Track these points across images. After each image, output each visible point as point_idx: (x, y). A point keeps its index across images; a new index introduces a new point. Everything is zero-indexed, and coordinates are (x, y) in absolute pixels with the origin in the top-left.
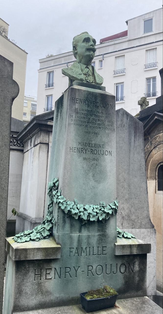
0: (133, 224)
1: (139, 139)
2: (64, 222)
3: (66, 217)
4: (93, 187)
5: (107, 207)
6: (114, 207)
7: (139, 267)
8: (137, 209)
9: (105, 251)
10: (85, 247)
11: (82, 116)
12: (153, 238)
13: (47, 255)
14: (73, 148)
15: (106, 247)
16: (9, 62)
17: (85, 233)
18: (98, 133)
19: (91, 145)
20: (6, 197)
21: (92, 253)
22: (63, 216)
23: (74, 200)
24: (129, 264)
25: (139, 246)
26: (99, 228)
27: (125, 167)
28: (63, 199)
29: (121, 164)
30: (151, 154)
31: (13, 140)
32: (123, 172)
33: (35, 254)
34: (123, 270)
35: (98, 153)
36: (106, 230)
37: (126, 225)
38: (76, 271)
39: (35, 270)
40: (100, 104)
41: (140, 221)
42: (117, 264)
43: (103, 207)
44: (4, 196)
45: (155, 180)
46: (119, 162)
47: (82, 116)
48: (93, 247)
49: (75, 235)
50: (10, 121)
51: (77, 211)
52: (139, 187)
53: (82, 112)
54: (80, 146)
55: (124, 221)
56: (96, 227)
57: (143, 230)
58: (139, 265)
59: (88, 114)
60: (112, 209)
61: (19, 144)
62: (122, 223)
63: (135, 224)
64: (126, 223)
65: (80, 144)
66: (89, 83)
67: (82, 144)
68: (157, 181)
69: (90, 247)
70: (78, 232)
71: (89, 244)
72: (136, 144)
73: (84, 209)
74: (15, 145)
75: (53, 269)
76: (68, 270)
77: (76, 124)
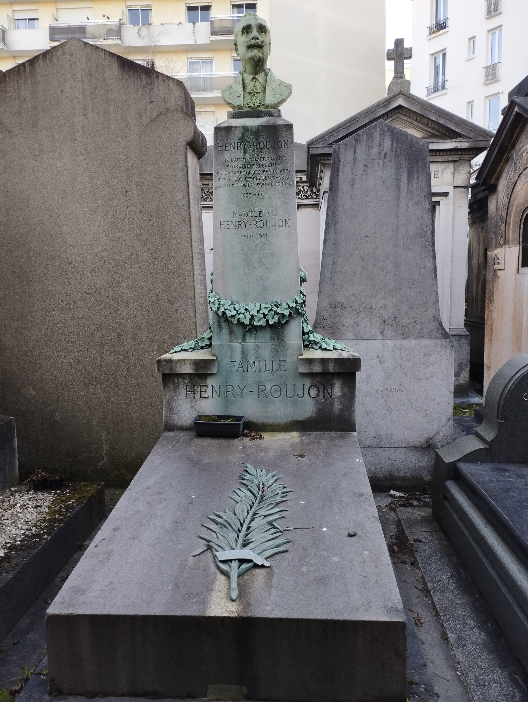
0: (404, 333)
1: (418, 176)
2: (220, 327)
3: (222, 321)
4: (260, 278)
5: (283, 306)
6: (294, 305)
7: (342, 391)
8: (413, 307)
9: (283, 366)
10: (252, 361)
11: (237, 169)
12: (447, 356)
13: (196, 370)
14: (225, 222)
15: (285, 361)
16: (176, 82)
17: (251, 342)
18: (264, 193)
19: (253, 214)
20: (193, 297)
21: (263, 368)
22: (218, 320)
23: (232, 298)
24: (324, 385)
25: (339, 361)
26: (273, 336)
27: (387, 234)
28: (214, 297)
29: (379, 228)
30: (515, 190)
31: (303, 187)
32: (383, 243)
33: (182, 367)
34: (313, 393)
35: (265, 225)
36: (285, 338)
37: (389, 333)
38: (242, 391)
39: (187, 386)
40: (265, 145)
41: (418, 327)
42: (303, 385)
43: (276, 305)
44: (190, 295)
45: (518, 245)
46: (375, 226)
47: (237, 169)
48: (265, 361)
49: (237, 345)
50: (186, 182)
51: (234, 313)
52: (418, 267)
53: (236, 163)
54: (236, 219)
55: (386, 327)
56: (267, 334)
57: (424, 342)
58: (342, 388)
59: (246, 165)
60: (289, 308)
61: (315, 193)
62: (382, 331)
63: (407, 331)
64: (390, 331)
65: (236, 215)
66: (253, 108)
67: (238, 215)
68: (521, 247)
69: (260, 361)
70: (240, 341)
71: (258, 356)
72: (412, 186)
73: (246, 309)
74: (308, 196)
75: (210, 387)
76: (230, 388)
77: (226, 185)
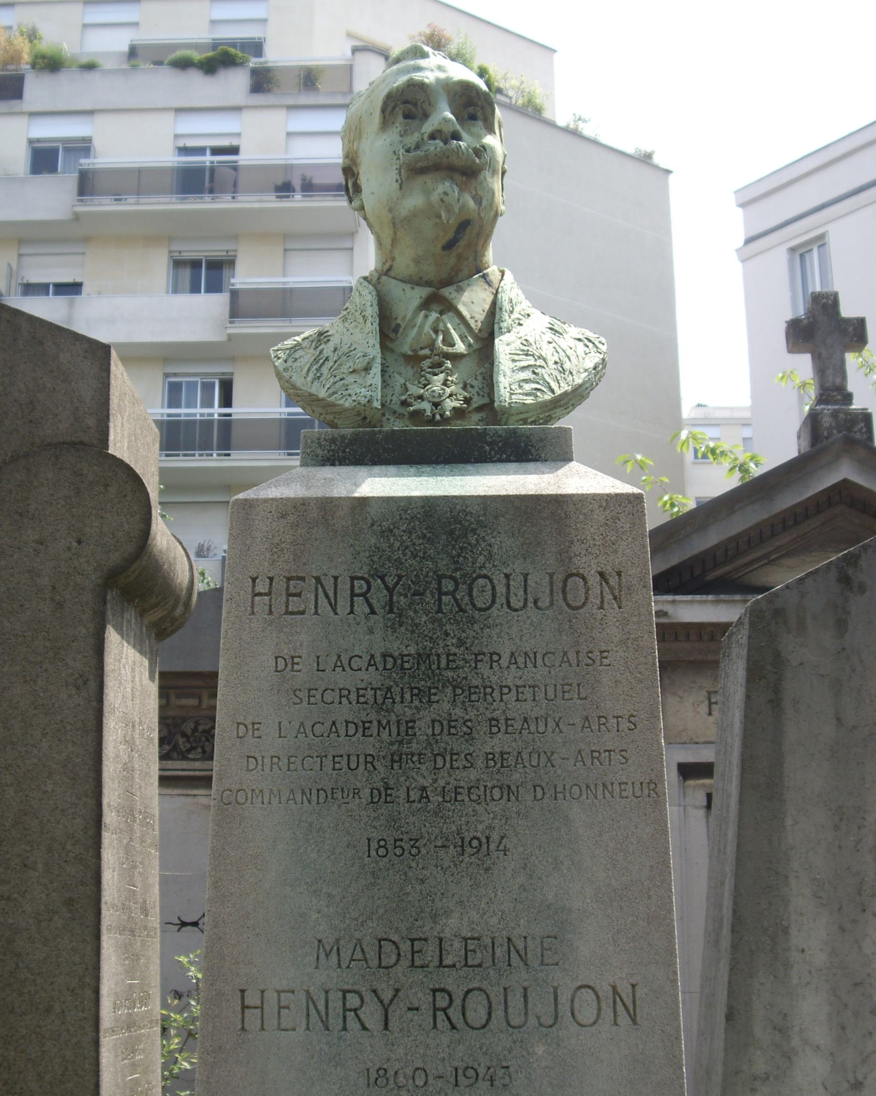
18: (495, 837)
19: (431, 952)
35: (498, 1013)
47: (344, 712)
53: (342, 679)
59: (396, 690)
65: (334, 958)
66: (431, 421)
67: (346, 956)
